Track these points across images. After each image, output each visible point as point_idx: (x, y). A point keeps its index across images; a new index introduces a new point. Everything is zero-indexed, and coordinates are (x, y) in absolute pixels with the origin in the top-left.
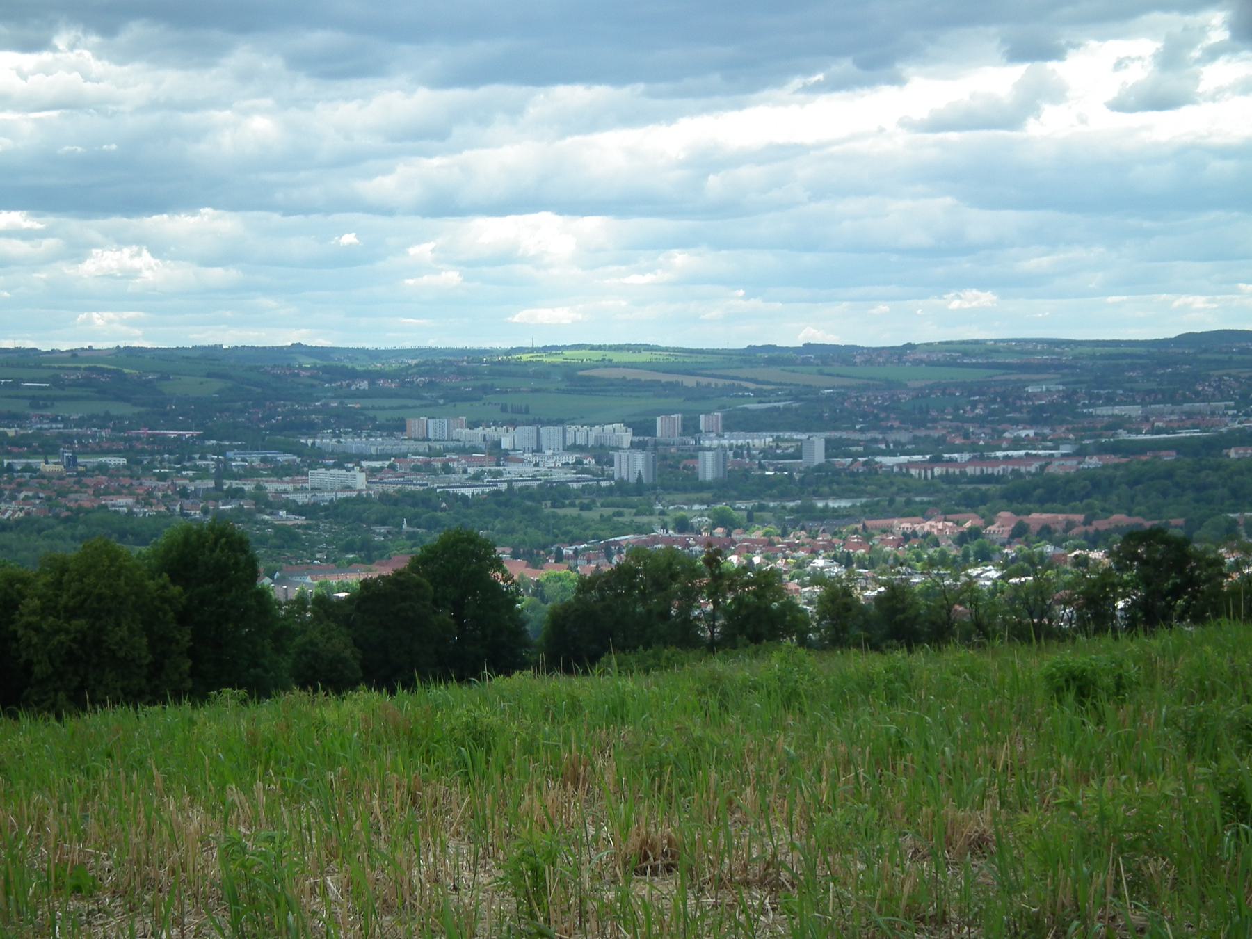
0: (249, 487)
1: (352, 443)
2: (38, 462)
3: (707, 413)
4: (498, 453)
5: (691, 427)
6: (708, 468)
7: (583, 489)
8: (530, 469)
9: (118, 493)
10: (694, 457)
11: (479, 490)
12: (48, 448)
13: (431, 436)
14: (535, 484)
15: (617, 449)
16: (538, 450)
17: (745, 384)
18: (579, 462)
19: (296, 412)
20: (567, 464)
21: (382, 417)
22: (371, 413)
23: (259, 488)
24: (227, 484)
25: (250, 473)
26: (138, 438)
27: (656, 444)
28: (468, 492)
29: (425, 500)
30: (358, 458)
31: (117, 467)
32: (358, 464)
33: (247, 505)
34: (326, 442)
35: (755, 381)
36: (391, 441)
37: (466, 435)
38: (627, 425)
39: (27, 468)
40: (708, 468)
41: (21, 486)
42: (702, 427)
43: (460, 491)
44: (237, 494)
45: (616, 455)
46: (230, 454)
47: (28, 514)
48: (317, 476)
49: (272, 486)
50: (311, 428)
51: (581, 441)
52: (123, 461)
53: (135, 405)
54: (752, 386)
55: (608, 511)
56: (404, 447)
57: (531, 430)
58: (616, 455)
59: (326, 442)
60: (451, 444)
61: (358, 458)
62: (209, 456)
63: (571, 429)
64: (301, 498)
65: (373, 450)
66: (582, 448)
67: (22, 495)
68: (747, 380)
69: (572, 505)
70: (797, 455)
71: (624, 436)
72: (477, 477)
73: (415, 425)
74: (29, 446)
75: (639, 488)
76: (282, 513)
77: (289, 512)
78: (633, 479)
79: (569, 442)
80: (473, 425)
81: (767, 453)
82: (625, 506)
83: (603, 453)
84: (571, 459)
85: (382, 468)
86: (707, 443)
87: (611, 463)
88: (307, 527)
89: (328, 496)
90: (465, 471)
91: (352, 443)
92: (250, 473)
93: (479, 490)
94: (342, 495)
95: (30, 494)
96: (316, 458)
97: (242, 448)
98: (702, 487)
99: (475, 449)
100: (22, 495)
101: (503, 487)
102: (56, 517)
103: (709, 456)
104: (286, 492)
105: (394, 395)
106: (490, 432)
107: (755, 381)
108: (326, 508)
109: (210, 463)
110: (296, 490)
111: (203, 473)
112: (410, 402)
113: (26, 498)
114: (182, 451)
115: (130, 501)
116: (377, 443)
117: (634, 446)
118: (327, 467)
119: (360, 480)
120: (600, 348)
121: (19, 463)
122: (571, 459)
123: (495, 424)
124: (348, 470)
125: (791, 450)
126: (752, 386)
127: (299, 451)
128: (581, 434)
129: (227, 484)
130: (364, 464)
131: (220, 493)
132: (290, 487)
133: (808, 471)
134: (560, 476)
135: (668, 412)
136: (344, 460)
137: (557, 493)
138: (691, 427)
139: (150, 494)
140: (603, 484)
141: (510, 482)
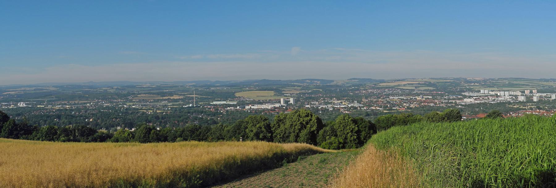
0: (454, 101)
1: (471, 94)
2: (417, 97)
3: (534, 90)
4: (497, 96)
5: (531, 92)
6: (535, 99)
7: (513, 102)
8: (503, 99)
9: (431, 103)
10: (532, 97)
11: (495, 102)
12: (418, 95)
13: (485, 93)
14: (505, 101)
15: (518, 96)
16: (505, 95)
17: (540, 85)
18: (512, 98)
19: (461, 89)
20: (510, 98)
21: (476, 89)
22: (474, 89)
23: (455, 102)
24: (450, 101)
25: (454, 99)
26: (434, 93)
27: (526, 95)
28: (492, 103)
29: (485, 104)
30: (472, 97)
31: (430, 98)
32: (473, 98)
33: (454, 105)
34: (467, 94)
35: (542, 85)
36: (478, 94)
37: (491, 93)
38: (520, 91)
39: (415, 99)
40: (535, 99)
41: (414, 102)
42: (533, 92)
43: (491, 102)
44: (452, 103)
45: (519, 97)
46: (450, 96)
47: (415, 106)
48: (465, 100)
49: (458, 101)
50: (464, 92)
51: (512, 94)
52: (431, 97)
53: (433, 88)
54: (542, 85)
55: (518, 106)
56: (481, 95)
57: (503, 92)
58: (519, 97)
59: (467, 94)
60: (489, 94)
61: (472, 97)
62: (446, 96)
63: (510, 92)
64: (463, 104)
65: (475, 95)
66: (512, 95)
67: (414, 103)
68: (541, 84)
69: (511, 105)
70: (551, 97)
71: (520, 94)
72: (494, 100)
73: (482, 91)
74: (415, 95)
75: (523, 102)
76: (460, 106)
77: (461, 106)
78: (522, 101)
79: (510, 94)
80: (492, 91)
81: (545, 97)
82: (521, 105)
83: (516, 96)
84: (511, 97)
85: (477, 99)
86: (534, 95)
87: (518, 98)
88: (465, 108)
89: (468, 103)
90: (492, 99)
91: (471, 94)
92: (454, 99)
93: (495, 102)
94: (470, 103)
95: (416, 103)
96: (465, 97)
97: (452, 95)
98: (535, 102)
99: (493, 95)
100: (414, 103)
101: (499, 102)
102: (420, 107)
103: (535, 97)
104: (460, 102)
105: (479, 86)
106: (496, 93)
107: (542, 85)
108: (467, 105)
109: (447, 97)
110: (462, 102)
111: (445, 99)
112: (482, 87)
113: (415, 104)
114: (442, 95)
115: (433, 104)
116: (476, 94)
117: (521, 95)
118: (467, 98)
119: (472, 100)
120: (514, 78)
121: (414, 98)
122: (511, 97)
123: (497, 91)
124: (471, 99)
125: (549, 96)
126: (542, 85)
127: (462, 95)
128: (512, 93)
129: (450, 101)
130: (474, 98)
131: (448, 103)
132: (461, 102)
133: (553, 100)
134: (509, 100)
135: (527, 90)
136: (470, 97)
137: (509, 103)
138: (531, 92)
139: (436, 102)
140: (517, 101)
141: (500, 101)
